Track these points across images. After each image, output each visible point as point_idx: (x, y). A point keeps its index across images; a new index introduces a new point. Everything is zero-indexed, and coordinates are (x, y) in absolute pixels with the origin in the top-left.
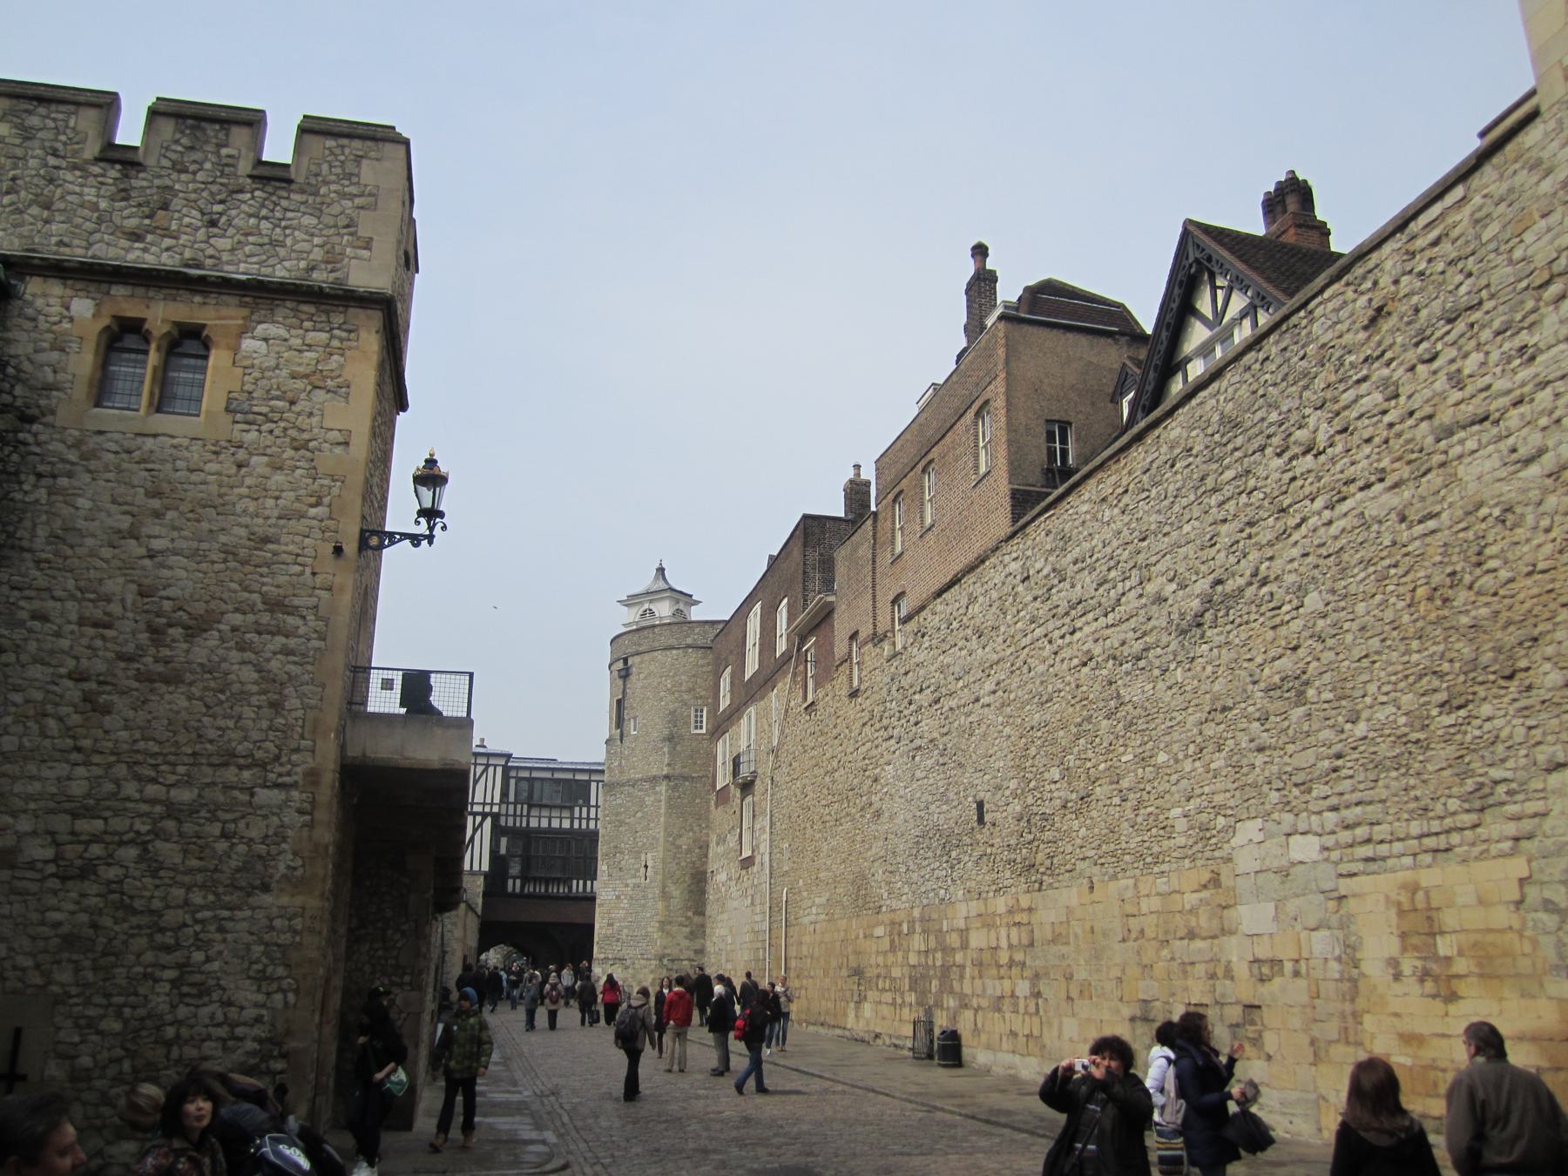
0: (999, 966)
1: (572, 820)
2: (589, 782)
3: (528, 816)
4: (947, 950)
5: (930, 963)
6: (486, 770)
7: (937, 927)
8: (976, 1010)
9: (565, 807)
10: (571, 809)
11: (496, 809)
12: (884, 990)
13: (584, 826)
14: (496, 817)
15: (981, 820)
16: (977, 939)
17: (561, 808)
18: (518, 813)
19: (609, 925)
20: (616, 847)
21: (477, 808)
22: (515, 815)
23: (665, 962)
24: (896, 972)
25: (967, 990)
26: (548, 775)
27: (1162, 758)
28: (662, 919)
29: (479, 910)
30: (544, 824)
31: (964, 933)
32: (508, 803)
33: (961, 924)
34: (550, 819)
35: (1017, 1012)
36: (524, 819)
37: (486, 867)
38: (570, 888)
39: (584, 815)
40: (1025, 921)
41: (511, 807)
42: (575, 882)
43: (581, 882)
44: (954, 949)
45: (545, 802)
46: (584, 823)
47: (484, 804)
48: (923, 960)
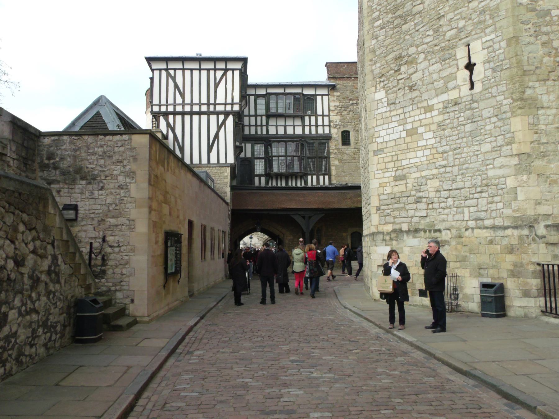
1: (303, 126)
2: (315, 95)
3: (267, 125)
6: (224, 74)
9: (297, 116)
10: (302, 118)
11: (236, 108)
13: (314, 132)
14: (238, 117)
17: (294, 117)
18: (259, 123)
19: (396, 179)
20: (400, 57)
21: (220, 108)
22: (256, 125)
23: (541, 230)
26: (281, 91)
28: (526, 149)
29: (228, 198)
30: (281, 131)
32: (250, 116)
34: (285, 126)
36: (264, 128)
37: (231, 160)
38: (306, 182)
39: (313, 123)
41: (253, 119)
42: (309, 177)
43: (315, 177)
45: (281, 111)
46: (313, 129)
47: (225, 104)
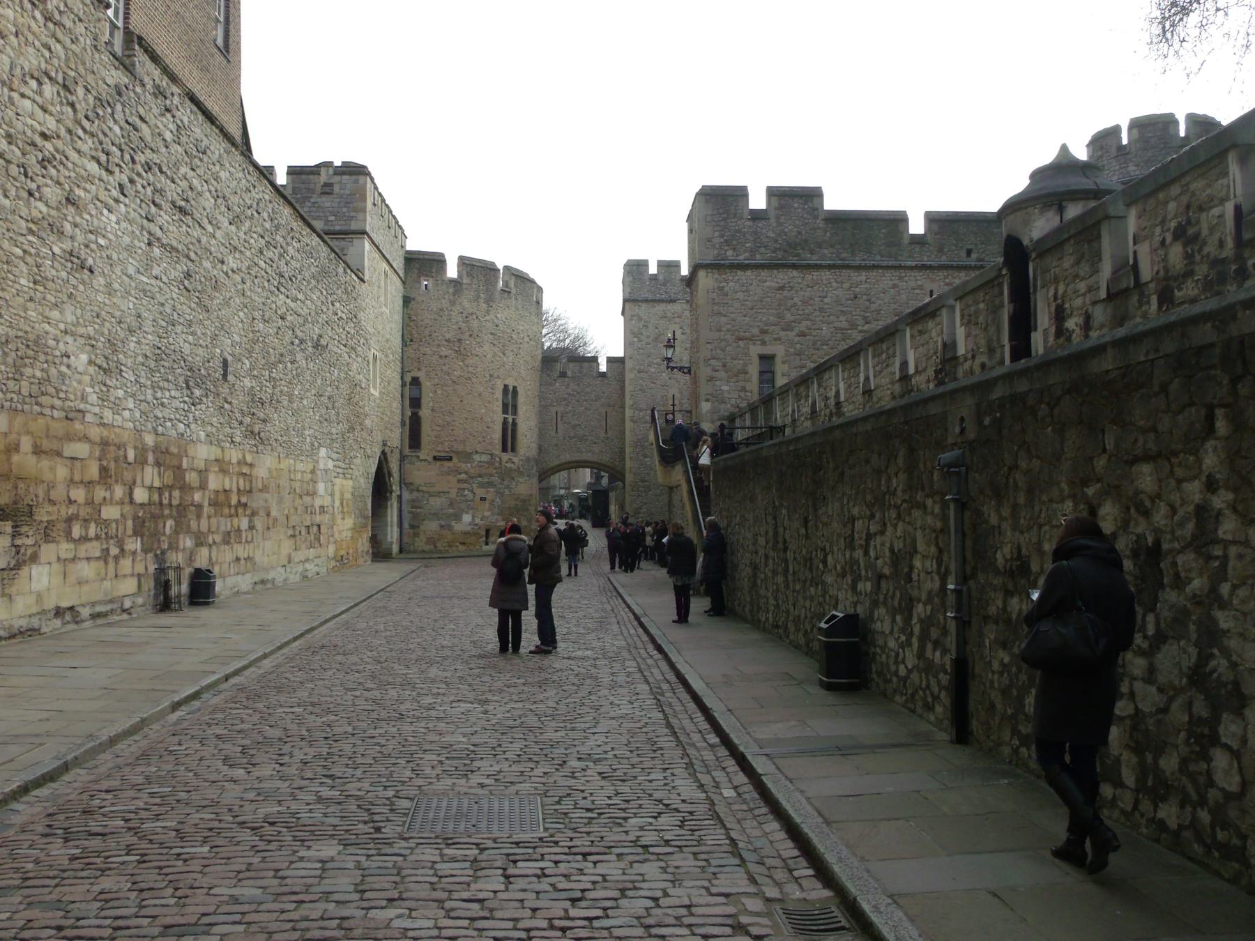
0: (230, 506)
4: (185, 488)
5: (165, 501)
7: (175, 462)
8: (210, 546)
12: (84, 539)
15: (225, 376)
16: (214, 482)
24: (110, 512)
25: (204, 528)
27: (305, 403)
31: (203, 473)
33: (202, 466)
35: (240, 542)
40: (248, 473)
44: (193, 488)
48: (156, 497)
